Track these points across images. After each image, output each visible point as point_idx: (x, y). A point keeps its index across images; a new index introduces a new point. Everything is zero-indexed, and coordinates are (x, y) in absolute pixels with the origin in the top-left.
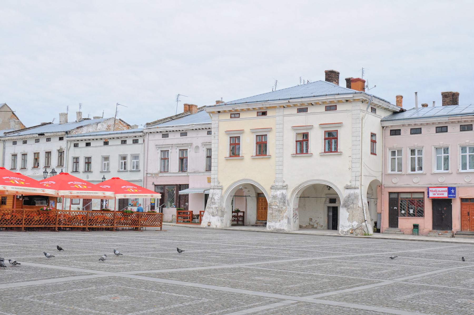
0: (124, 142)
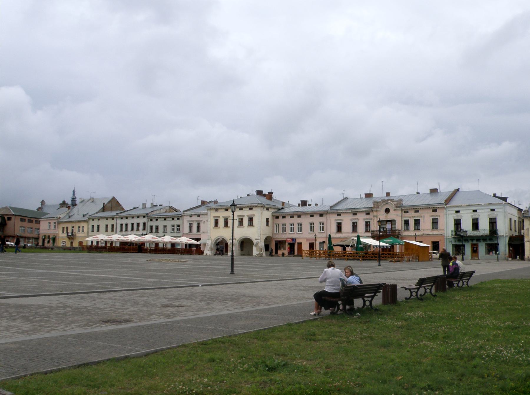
0: (173, 219)
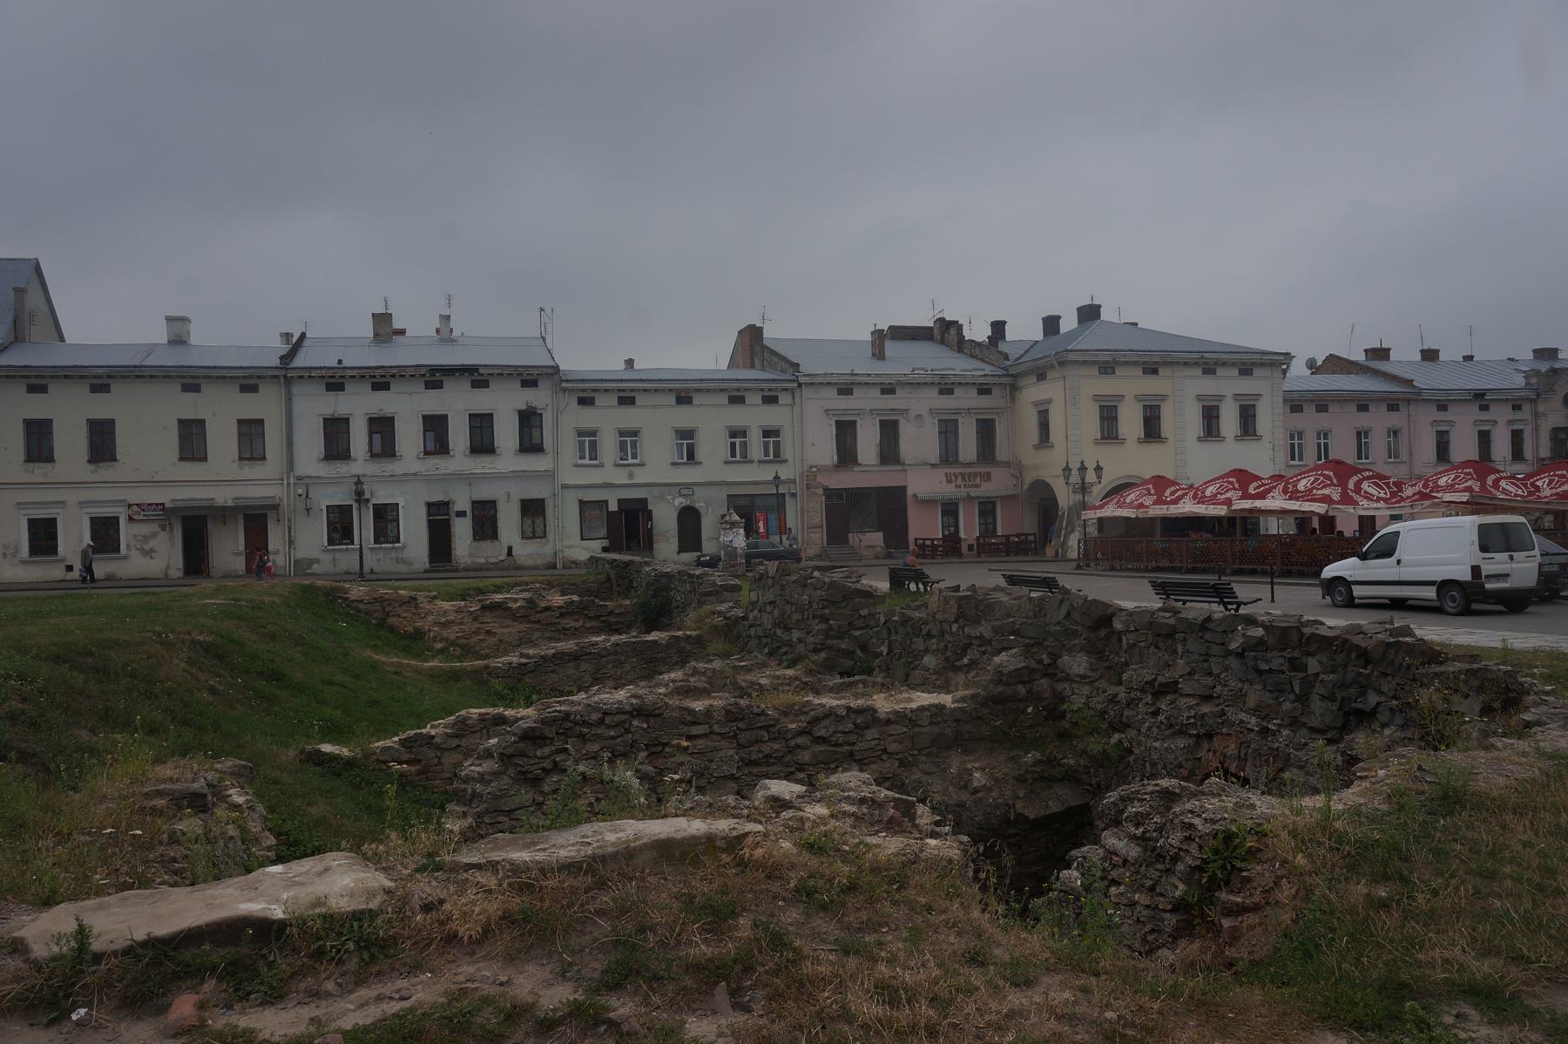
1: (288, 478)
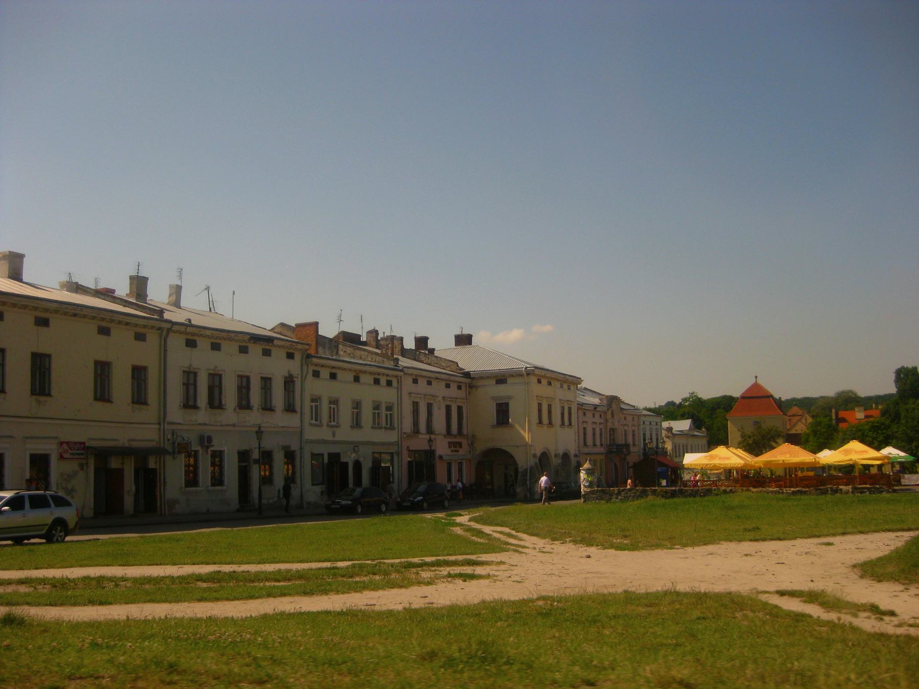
0: (377, 382)
1: (164, 423)
